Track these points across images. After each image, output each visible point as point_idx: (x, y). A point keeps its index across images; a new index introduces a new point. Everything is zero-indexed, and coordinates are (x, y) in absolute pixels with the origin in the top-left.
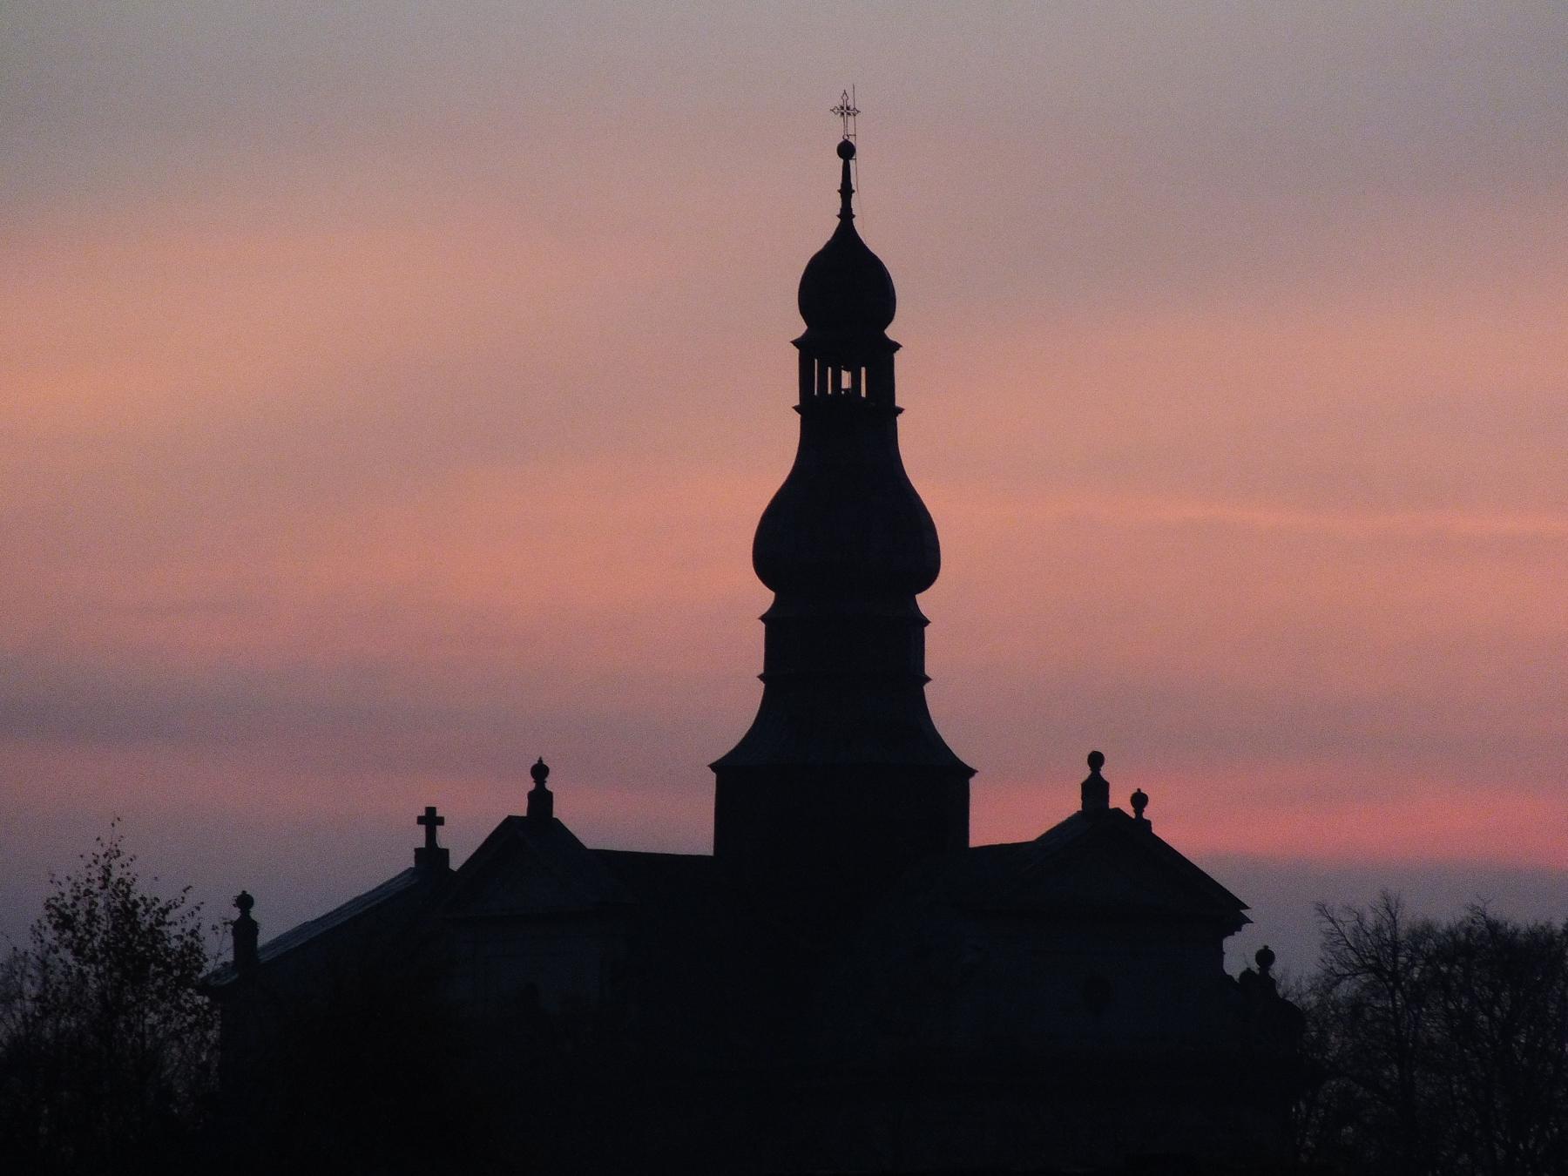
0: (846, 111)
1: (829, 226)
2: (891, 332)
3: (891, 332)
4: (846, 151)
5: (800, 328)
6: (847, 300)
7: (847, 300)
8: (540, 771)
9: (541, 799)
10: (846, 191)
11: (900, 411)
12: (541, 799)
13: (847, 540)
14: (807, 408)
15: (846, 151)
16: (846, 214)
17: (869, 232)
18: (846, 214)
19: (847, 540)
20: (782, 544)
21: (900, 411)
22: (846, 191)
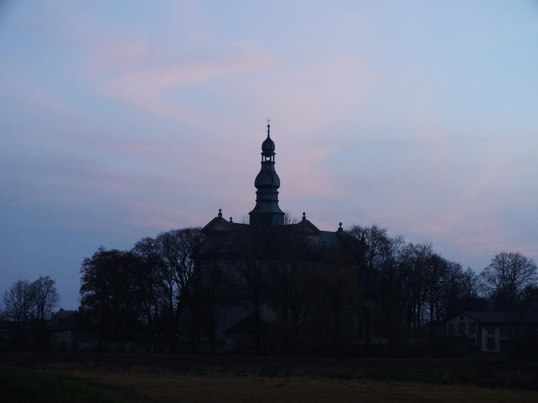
2: (275, 152)
3: (275, 152)
4: (269, 126)
5: (262, 152)
6: (268, 147)
7: (268, 147)
8: (220, 210)
9: (220, 214)
10: (269, 132)
12: (220, 214)
13: (267, 183)
14: (263, 163)
15: (269, 126)
16: (269, 135)
18: (269, 135)
19: (267, 183)
20: (259, 182)
22: (269, 132)
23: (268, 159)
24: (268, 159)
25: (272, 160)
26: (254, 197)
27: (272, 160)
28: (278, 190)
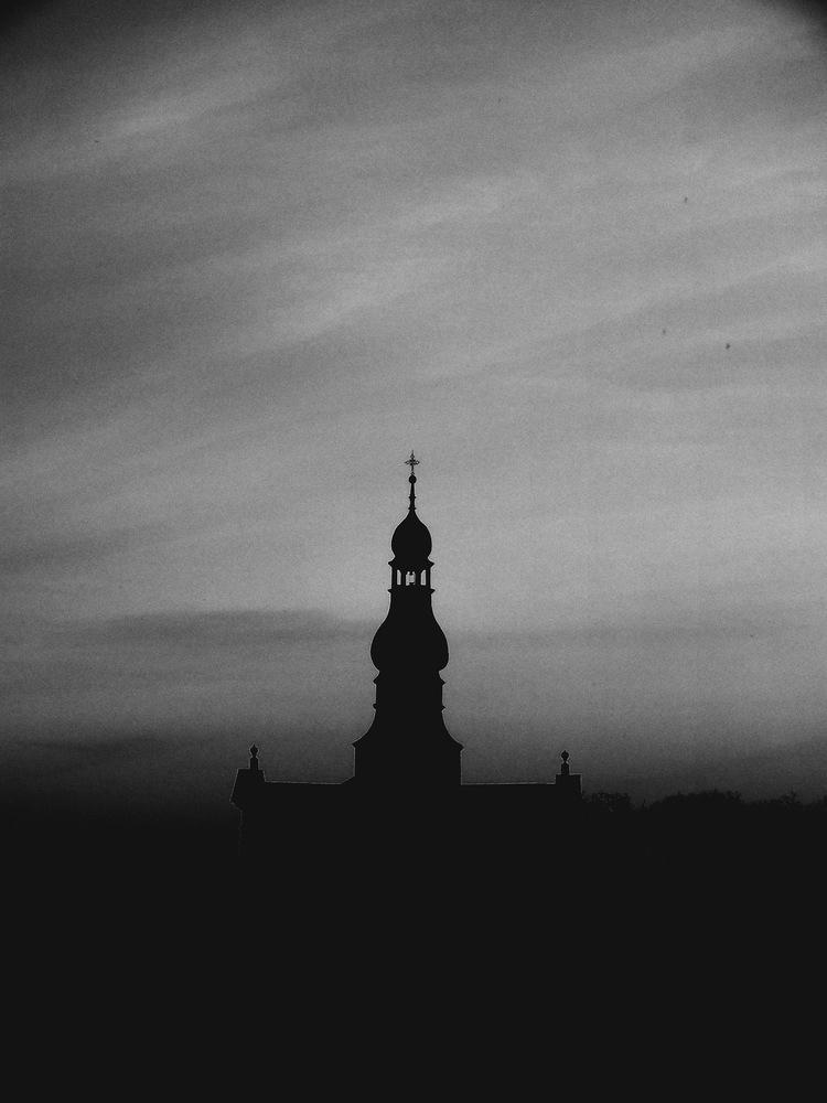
0: (413, 462)
1: (402, 515)
2: (431, 558)
4: (413, 480)
6: (412, 544)
7: (412, 544)
10: (412, 498)
11: (433, 591)
12: (254, 761)
14: (396, 591)
15: (413, 480)
16: (412, 508)
17: (422, 515)
18: (412, 508)
21: (433, 591)
22: (412, 498)
23: (410, 579)
24: (410, 579)
25: (423, 583)
26: (371, 689)
27: (423, 583)
28: (443, 673)
